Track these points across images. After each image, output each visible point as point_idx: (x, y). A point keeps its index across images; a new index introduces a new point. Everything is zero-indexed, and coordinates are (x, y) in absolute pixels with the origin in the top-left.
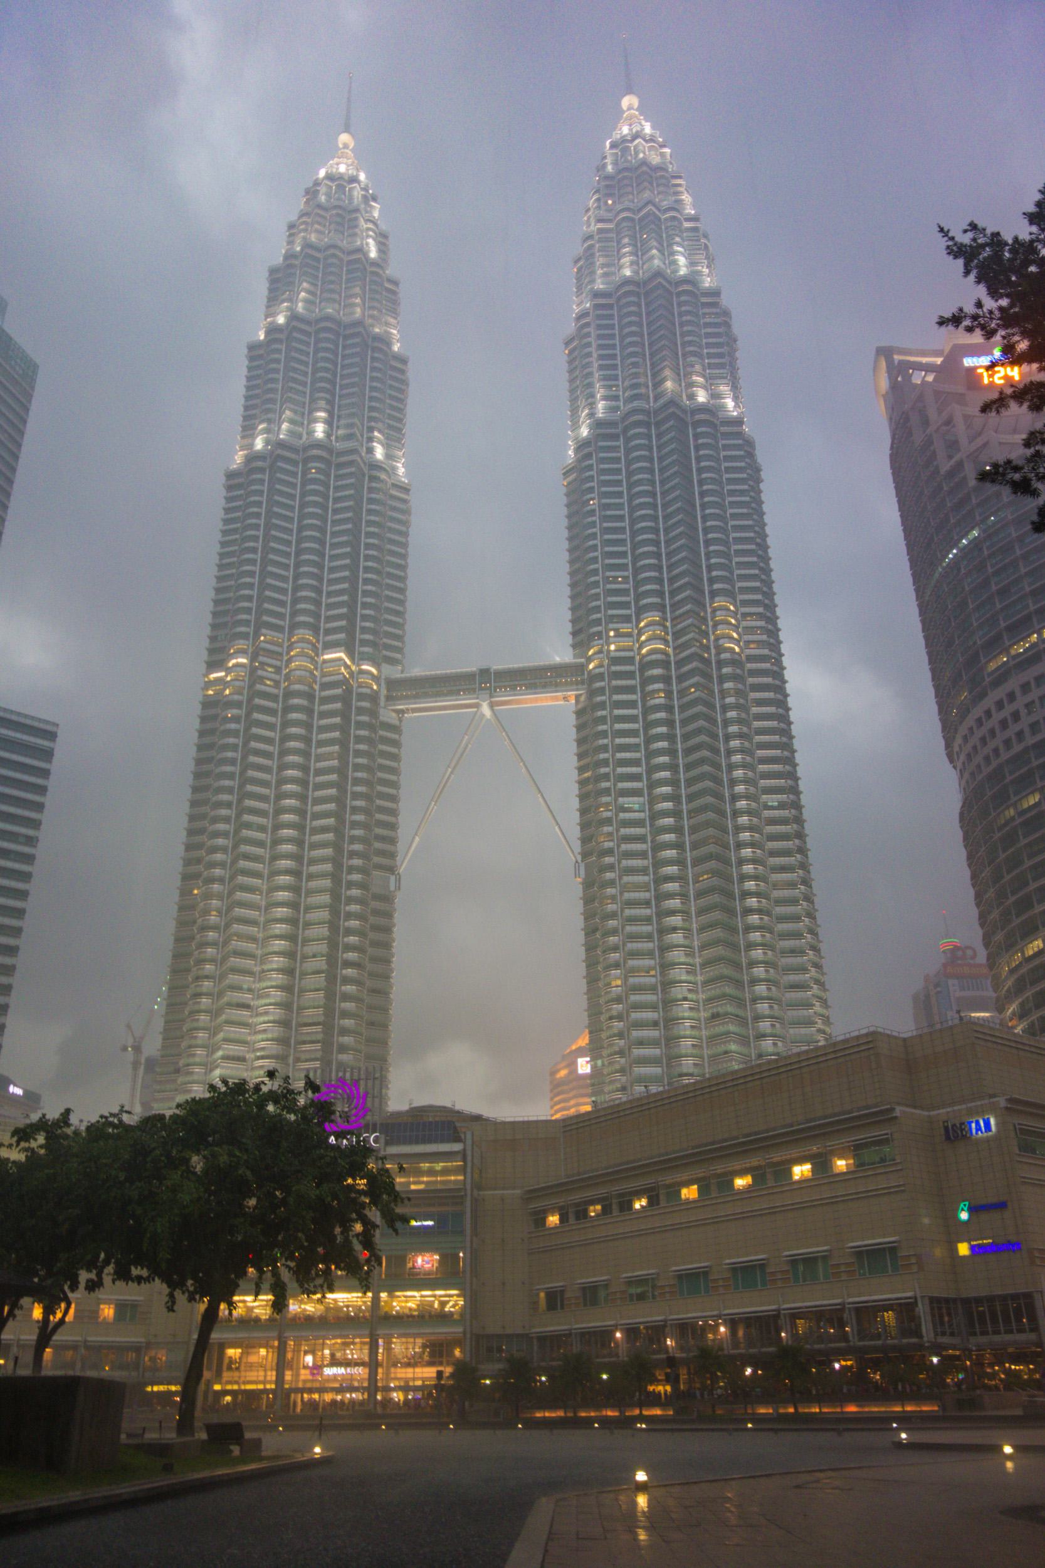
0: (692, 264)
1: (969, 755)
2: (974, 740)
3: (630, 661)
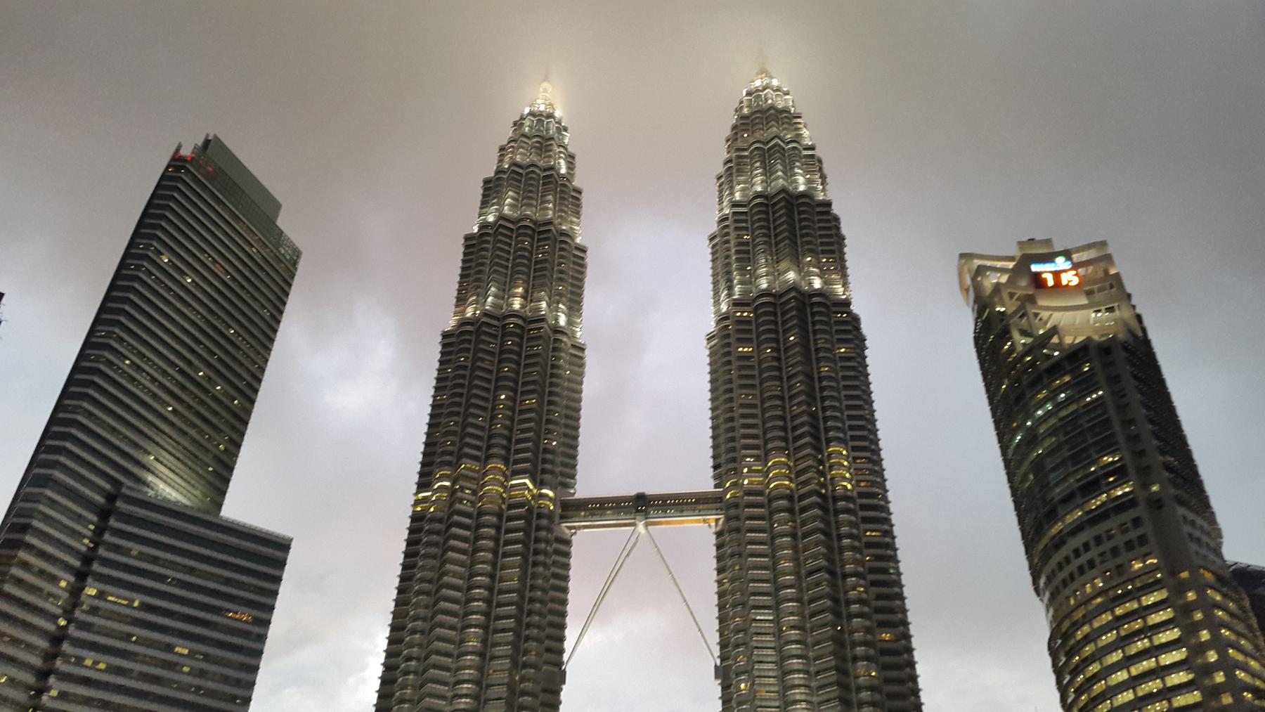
0: (809, 181)
1: (1052, 594)
2: (1057, 582)
3: (760, 493)
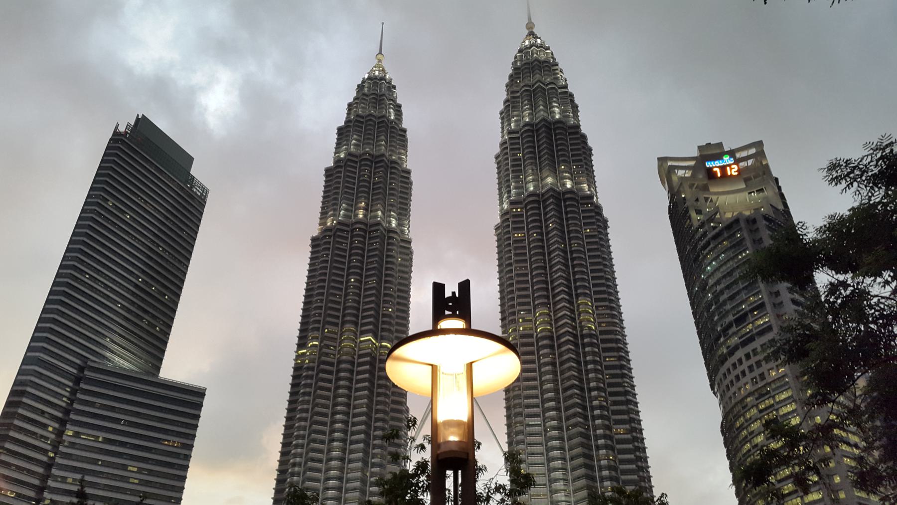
0: (563, 112)
2: (723, 387)
3: (531, 336)
